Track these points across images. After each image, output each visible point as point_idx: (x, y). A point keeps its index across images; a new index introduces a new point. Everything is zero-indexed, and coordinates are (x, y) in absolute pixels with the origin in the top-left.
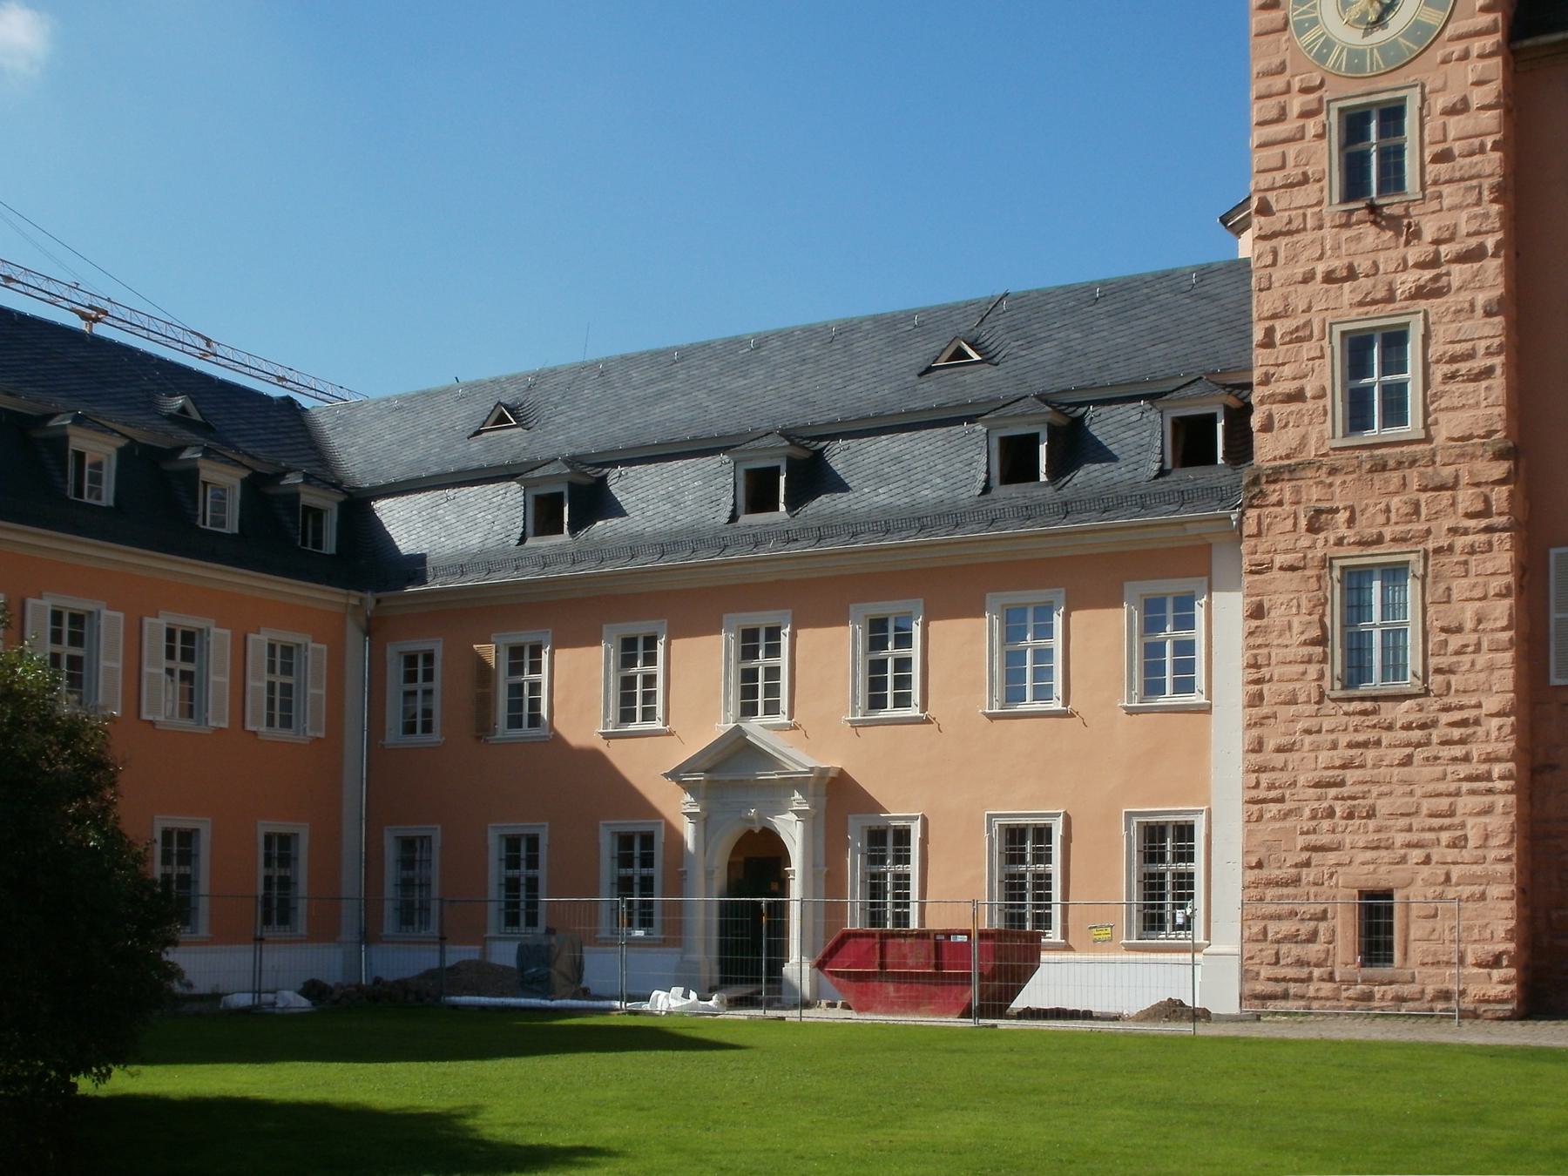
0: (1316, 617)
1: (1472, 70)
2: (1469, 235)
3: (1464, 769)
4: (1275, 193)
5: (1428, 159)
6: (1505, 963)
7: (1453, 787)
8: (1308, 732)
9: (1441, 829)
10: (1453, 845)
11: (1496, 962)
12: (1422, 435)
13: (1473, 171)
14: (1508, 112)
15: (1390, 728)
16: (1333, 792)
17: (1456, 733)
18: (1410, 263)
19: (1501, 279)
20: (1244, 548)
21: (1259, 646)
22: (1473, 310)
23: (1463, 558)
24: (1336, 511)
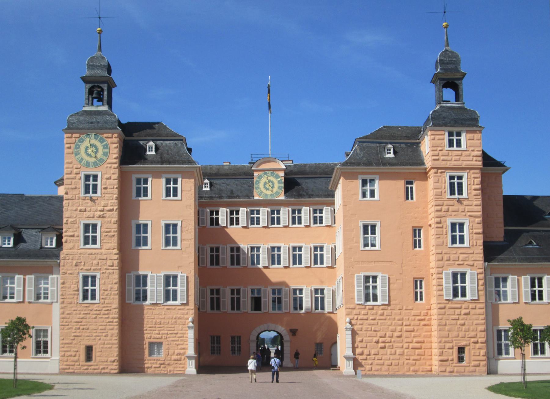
0: (76, 285)
1: (113, 171)
2: (110, 206)
3: (108, 320)
4: (69, 190)
5: (102, 188)
6: (116, 361)
7: (105, 324)
8: (74, 310)
9: (103, 333)
10: (105, 336)
11: (114, 361)
12: (100, 247)
13: (112, 193)
14: (119, 181)
15: (92, 310)
16: (80, 324)
17: (106, 312)
18: (98, 210)
19: (117, 216)
21: (64, 291)
23: (108, 275)
24: (81, 262)
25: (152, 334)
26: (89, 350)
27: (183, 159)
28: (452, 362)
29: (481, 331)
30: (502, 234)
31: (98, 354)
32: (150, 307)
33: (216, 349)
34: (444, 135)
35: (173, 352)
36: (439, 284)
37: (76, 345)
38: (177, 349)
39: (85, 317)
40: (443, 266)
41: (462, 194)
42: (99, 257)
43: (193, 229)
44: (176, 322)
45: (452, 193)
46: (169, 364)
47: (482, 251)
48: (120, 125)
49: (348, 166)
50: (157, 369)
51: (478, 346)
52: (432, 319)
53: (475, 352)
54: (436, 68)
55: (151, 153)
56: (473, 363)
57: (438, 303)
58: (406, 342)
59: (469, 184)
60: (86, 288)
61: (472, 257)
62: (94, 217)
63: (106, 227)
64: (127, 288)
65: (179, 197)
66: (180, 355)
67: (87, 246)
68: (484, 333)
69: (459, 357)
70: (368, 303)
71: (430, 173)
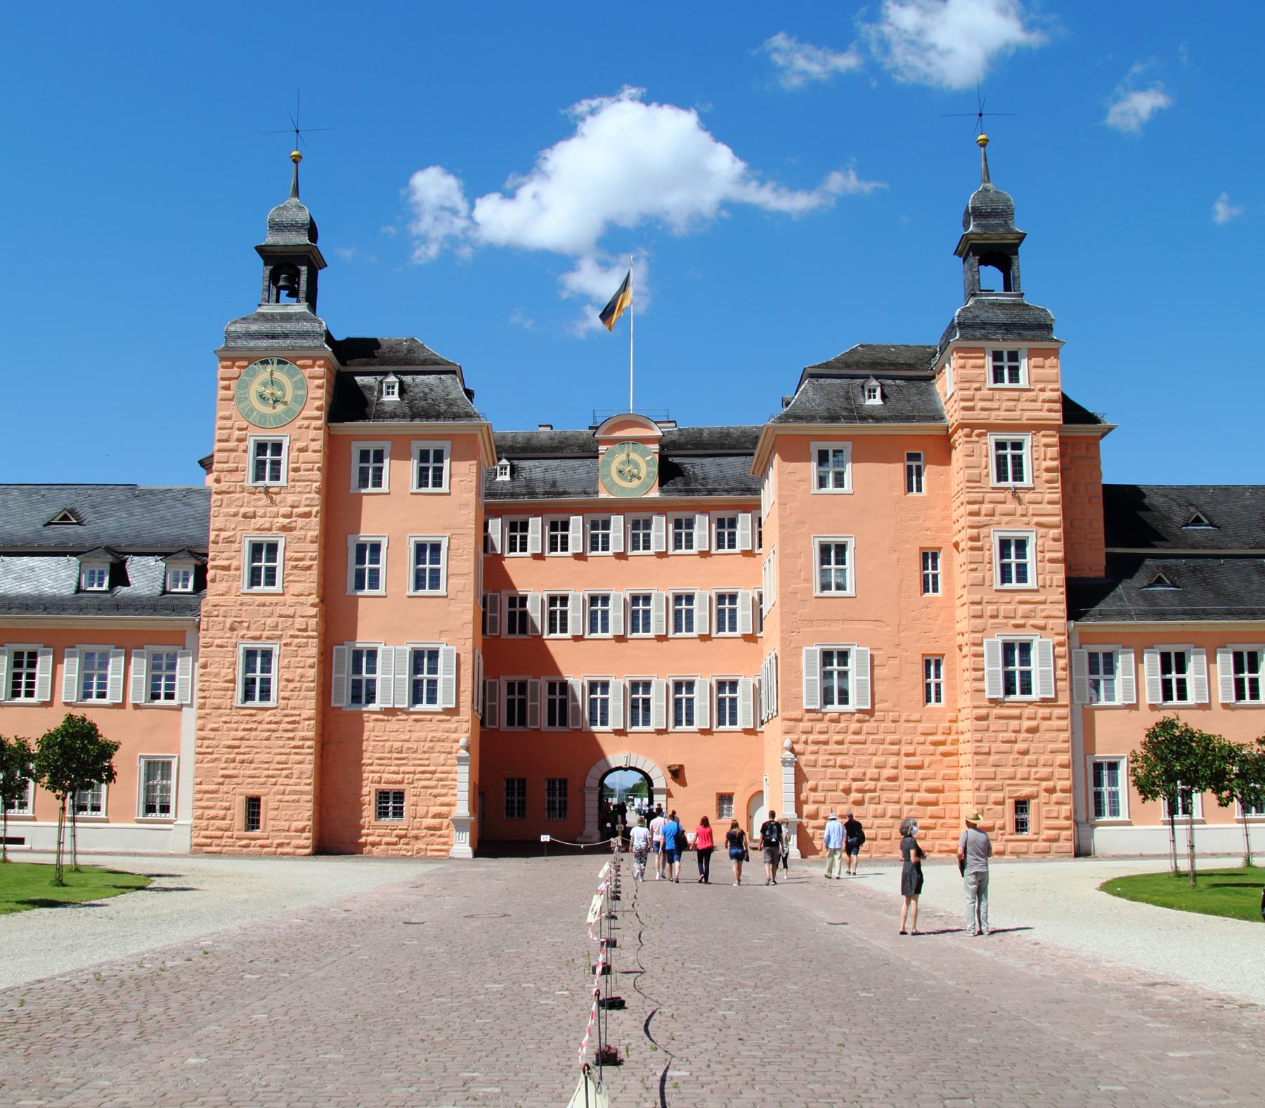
0: (231, 670)
1: (313, 433)
3: (293, 743)
5: (290, 469)
7: (288, 751)
8: (225, 722)
9: (282, 769)
10: (287, 777)
11: (303, 830)
13: (309, 478)
15: (260, 723)
16: (236, 750)
17: (290, 727)
19: (318, 527)
20: (202, 633)
21: (205, 681)
22: (305, 539)
23: (296, 649)
24: (243, 622)
25: (383, 772)
26: (253, 804)
27: (455, 409)
28: (1001, 832)
29: (1062, 766)
30: (1102, 562)
31: (272, 814)
32: (381, 717)
33: (516, 805)
34: (984, 358)
35: (425, 811)
36: (976, 667)
37: (226, 796)
38: (434, 805)
39: (247, 737)
40: (984, 629)
41: (1021, 479)
42: (279, 610)
43: (473, 553)
44: (432, 748)
45: (1002, 476)
46: (416, 838)
47: (1063, 597)
48: (329, 339)
49: (790, 422)
50: (391, 847)
51: (1055, 797)
52: (961, 741)
53: (1049, 810)
54: (966, 225)
55: (392, 398)
56: (1047, 834)
57: (974, 707)
58: (908, 791)
59: (1037, 459)
60: (250, 675)
61: (1043, 610)
62: (270, 529)
63: (296, 550)
64: (334, 675)
65: (445, 488)
66: (439, 818)
67: (256, 589)
68: (1067, 772)
69: (1017, 819)
70: (829, 707)
71: (956, 437)
